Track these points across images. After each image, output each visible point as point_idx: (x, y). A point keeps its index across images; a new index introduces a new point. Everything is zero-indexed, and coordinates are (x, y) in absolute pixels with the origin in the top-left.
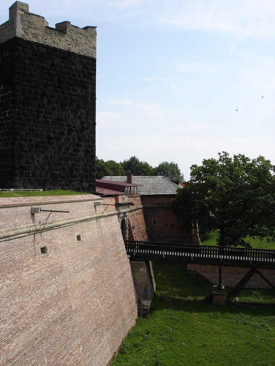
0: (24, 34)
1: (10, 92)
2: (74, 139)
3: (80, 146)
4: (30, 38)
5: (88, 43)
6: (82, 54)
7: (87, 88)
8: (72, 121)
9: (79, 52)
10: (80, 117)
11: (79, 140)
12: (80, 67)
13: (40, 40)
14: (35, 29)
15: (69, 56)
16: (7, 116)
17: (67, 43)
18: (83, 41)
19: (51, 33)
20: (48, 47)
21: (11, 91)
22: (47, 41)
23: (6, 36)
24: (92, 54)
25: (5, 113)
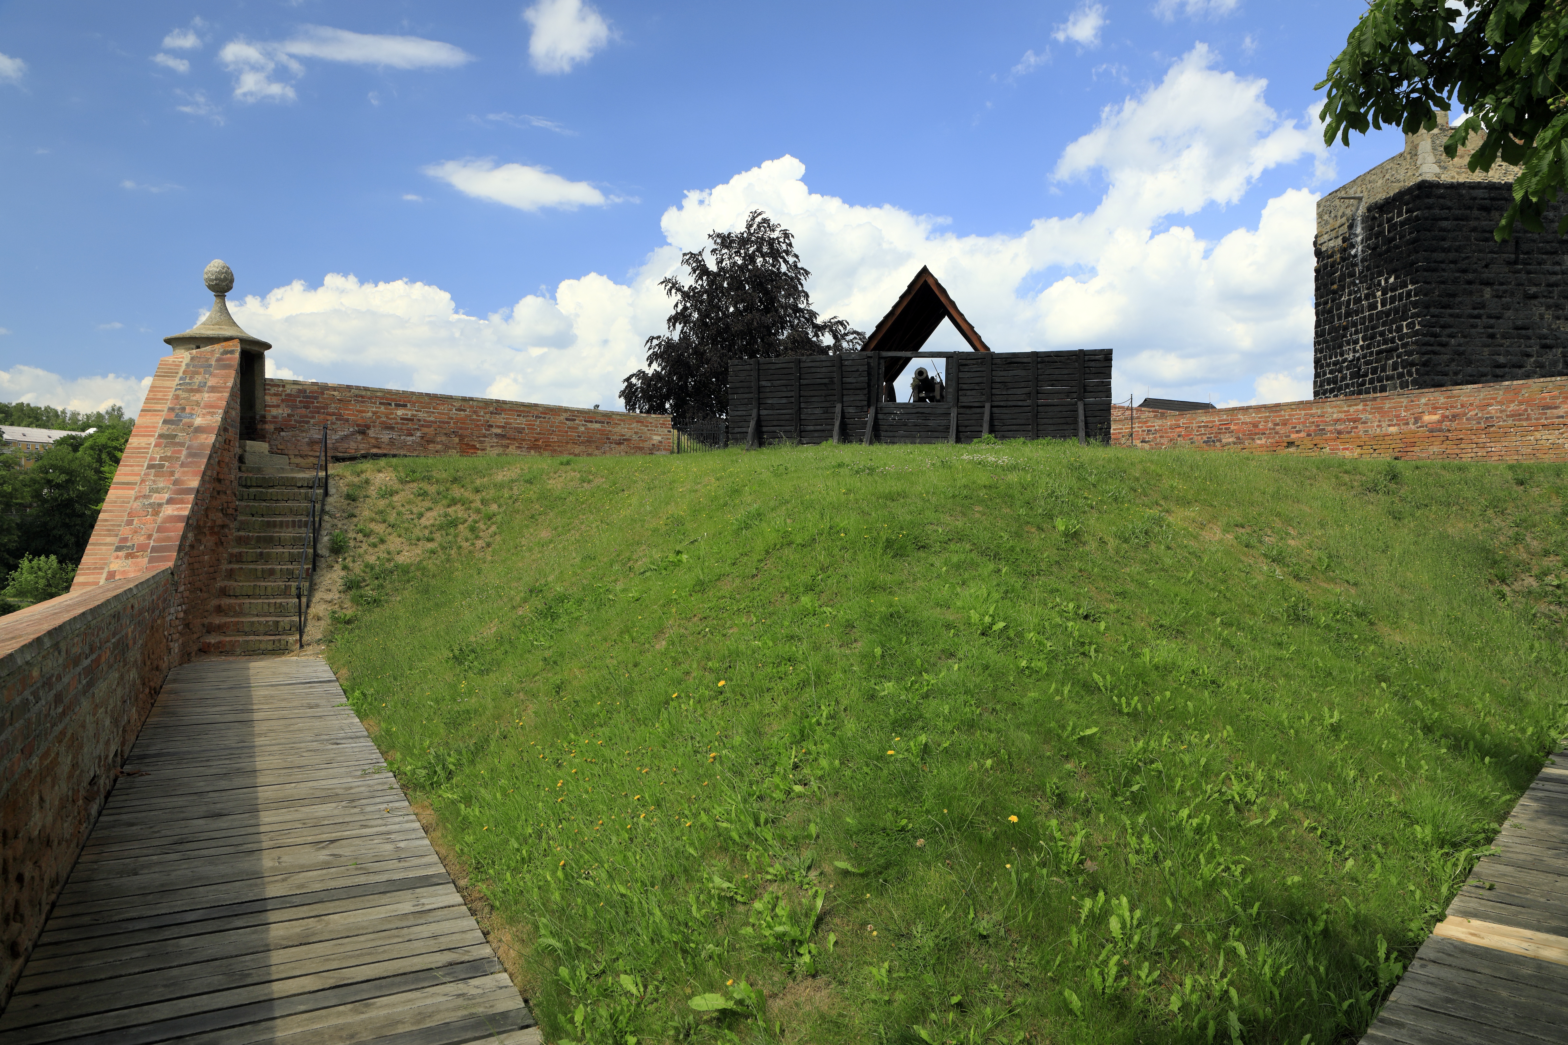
1: (1410, 287)
4: (1453, 177)
8: (1550, 326)
16: (1405, 331)
21: (1412, 283)
23: (1399, 181)
25: (1399, 329)
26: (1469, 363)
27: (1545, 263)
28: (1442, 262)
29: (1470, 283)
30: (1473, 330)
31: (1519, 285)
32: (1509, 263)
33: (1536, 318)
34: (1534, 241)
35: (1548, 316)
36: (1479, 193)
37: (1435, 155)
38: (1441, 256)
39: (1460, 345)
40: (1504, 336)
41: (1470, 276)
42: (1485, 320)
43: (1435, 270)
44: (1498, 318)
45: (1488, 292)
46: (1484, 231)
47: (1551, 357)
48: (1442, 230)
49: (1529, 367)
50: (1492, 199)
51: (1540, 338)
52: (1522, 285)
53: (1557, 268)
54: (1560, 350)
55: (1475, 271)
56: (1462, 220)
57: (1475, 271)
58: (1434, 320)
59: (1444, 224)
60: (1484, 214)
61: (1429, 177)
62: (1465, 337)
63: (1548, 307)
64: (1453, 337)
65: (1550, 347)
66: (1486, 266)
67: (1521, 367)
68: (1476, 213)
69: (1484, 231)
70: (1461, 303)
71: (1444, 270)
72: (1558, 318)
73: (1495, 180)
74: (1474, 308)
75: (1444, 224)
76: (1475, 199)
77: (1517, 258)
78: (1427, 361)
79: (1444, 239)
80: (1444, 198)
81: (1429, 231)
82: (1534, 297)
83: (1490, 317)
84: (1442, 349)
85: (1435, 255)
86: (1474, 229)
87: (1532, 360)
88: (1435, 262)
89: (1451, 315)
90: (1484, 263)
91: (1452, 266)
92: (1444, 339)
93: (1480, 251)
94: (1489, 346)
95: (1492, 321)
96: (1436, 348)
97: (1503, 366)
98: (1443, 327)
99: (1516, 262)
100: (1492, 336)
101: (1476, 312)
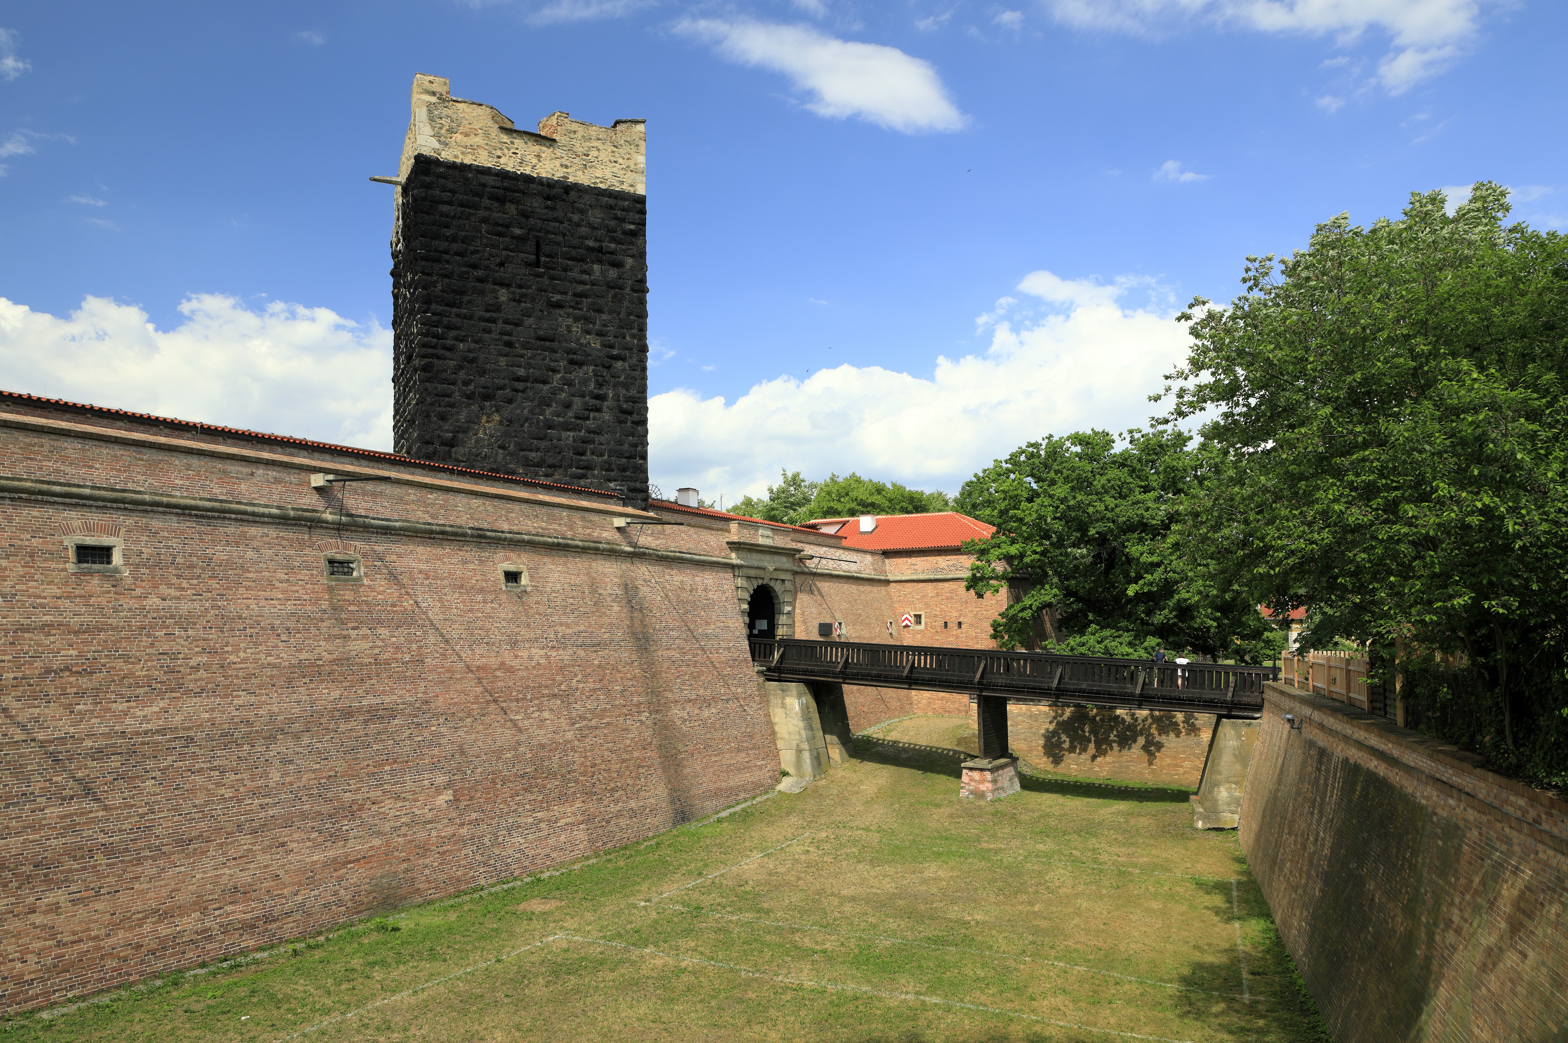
0: (437, 145)
2: (585, 382)
3: (602, 398)
4: (456, 157)
5: (620, 161)
6: (602, 186)
7: (618, 265)
9: (595, 183)
10: (600, 334)
11: (600, 385)
12: (596, 216)
13: (484, 160)
14: (466, 135)
15: (567, 193)
17: (557, 163)
18: (603, 156)
19: (512, 143)
20: (504, 175)
22: (502, 161)
24: (632, 186)
26: (483, 373)
27: (571, 270)
28: (446, 252)
29: (480, 280)
30: (486, 336)
31: (541, 290)
32: (528, 264)
33: (563, 330)
34: (558, 244)
35: (576, 329)
36: (490, 180)
37: (433, 128)
38: (444, 245)
39: (470, 351)
40: (525, 346)
41: (480, 273)
42: (500, 325)
43: (437, 261)
44: (517, 325)
45: (503, 295)
46: (497, 224)
47: (581, 375)
48: (442, 215)
49: (555, 384)
50: (506, 189)
51: (568, 353)
52: (545, 291)
53: (585, 277)
54: (592, 368)
55: (487, 268)
56: (470, 207)
57: (487, 268)
58: (435, 318)
59: (445, 208)
60: (497, 205)
61: (426, 152)
62: (477, 342)
63: (577, 319)
64: (461, 341)
65: (580, 364)
66: (502, 264)
67: (545, 382)
68: (486, 202)
69: (497, 224)
70: (470, 302)
71: (447, 262)
72: (588, 332)
73: (509, 169)
74: (487, 311)
75: (445, 208)
76: (485, 185)
77: (538, 260)
78: (426, 365)
79: (447, 226)
80: (445, 178)
81: (428, 214)
82: (559, 305)
83: (506, 322)
84: (448, 354)
85: (435, 243)
86: (485, 220)
87: (559, 376)
88: (436, 251)
89: (458, 315)
90: (498, 260)
91: (458, 258)
92: (449, 342)
93: (493, 246)
94: (506, 355)
95: (509, 327)
96: (441, 352)
97: (525, 380)
98: (449, 327)
99: (537, 264)
100: (509, 344)
101: (488, 315)
